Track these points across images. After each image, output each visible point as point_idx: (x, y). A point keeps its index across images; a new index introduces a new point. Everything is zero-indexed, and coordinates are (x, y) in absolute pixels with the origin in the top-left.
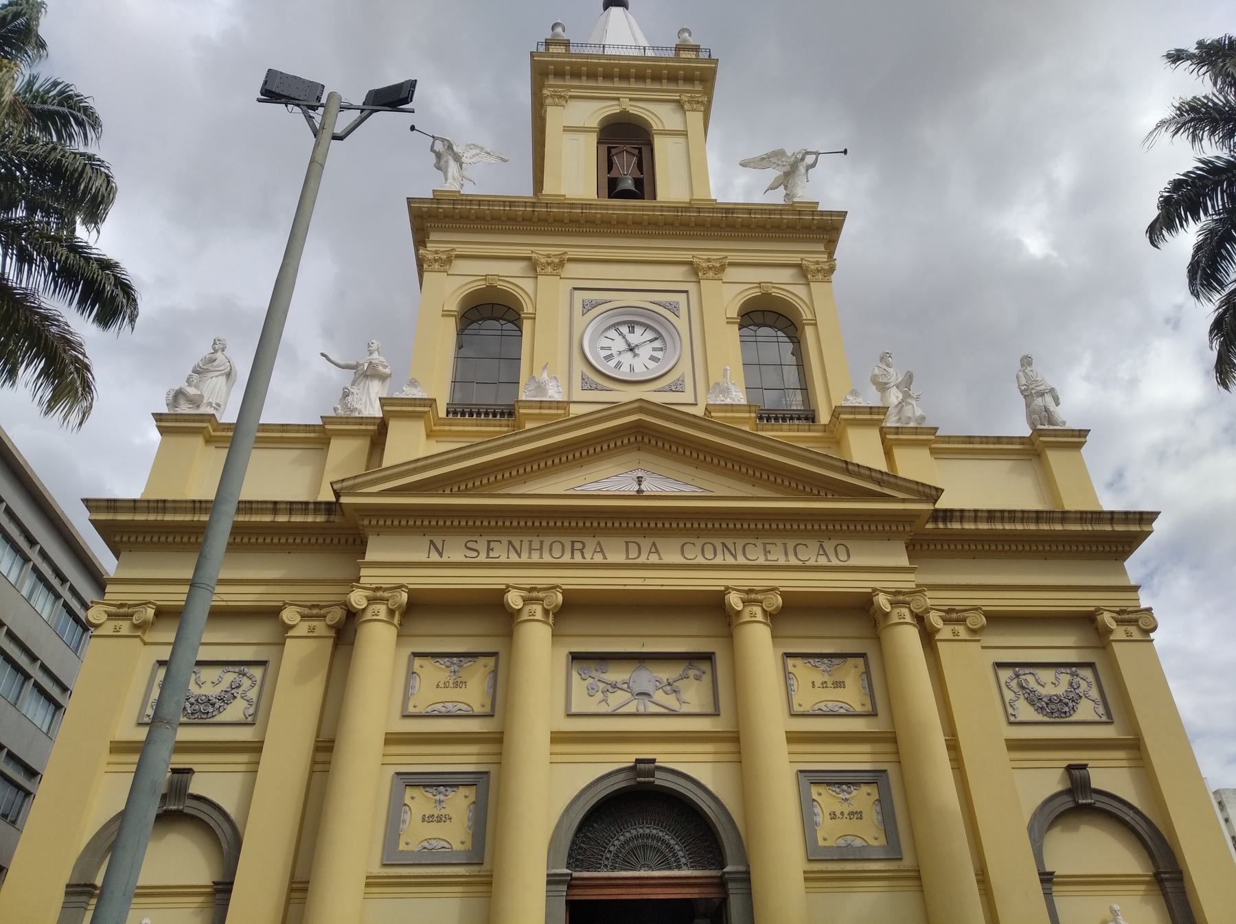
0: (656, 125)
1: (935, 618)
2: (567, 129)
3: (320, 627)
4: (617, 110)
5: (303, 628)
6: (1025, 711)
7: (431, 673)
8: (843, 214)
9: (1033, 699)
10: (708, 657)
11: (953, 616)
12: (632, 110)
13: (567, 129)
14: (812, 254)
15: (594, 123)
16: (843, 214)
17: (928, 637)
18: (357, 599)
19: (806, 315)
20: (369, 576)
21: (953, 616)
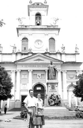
0: (42, 15)
1: (62, 71)
2: (32, 15)
3: (14, 72)
4: (37, 12)
5: (13, 72)
6: (69, 78)
7: (23, 76)
8: (60, 28)
9: (70, 77)
10: (44, 75)
11: (64, 71)
12: (39, 12)
13: (32, 15)
14: (57, 32)
15: (35, 15)
16: (60, 28)
17: (62, 72)
18: (17, 71)
19: (55, 40)
20: (18, 69)
21: (64, 71)
